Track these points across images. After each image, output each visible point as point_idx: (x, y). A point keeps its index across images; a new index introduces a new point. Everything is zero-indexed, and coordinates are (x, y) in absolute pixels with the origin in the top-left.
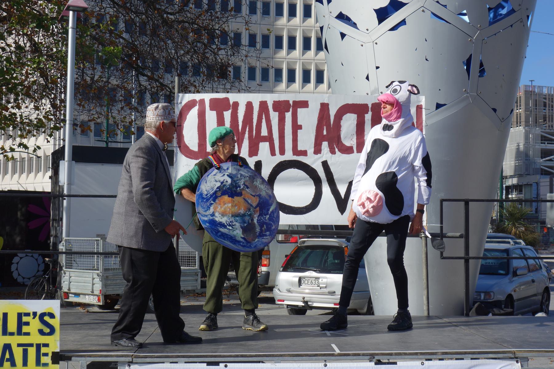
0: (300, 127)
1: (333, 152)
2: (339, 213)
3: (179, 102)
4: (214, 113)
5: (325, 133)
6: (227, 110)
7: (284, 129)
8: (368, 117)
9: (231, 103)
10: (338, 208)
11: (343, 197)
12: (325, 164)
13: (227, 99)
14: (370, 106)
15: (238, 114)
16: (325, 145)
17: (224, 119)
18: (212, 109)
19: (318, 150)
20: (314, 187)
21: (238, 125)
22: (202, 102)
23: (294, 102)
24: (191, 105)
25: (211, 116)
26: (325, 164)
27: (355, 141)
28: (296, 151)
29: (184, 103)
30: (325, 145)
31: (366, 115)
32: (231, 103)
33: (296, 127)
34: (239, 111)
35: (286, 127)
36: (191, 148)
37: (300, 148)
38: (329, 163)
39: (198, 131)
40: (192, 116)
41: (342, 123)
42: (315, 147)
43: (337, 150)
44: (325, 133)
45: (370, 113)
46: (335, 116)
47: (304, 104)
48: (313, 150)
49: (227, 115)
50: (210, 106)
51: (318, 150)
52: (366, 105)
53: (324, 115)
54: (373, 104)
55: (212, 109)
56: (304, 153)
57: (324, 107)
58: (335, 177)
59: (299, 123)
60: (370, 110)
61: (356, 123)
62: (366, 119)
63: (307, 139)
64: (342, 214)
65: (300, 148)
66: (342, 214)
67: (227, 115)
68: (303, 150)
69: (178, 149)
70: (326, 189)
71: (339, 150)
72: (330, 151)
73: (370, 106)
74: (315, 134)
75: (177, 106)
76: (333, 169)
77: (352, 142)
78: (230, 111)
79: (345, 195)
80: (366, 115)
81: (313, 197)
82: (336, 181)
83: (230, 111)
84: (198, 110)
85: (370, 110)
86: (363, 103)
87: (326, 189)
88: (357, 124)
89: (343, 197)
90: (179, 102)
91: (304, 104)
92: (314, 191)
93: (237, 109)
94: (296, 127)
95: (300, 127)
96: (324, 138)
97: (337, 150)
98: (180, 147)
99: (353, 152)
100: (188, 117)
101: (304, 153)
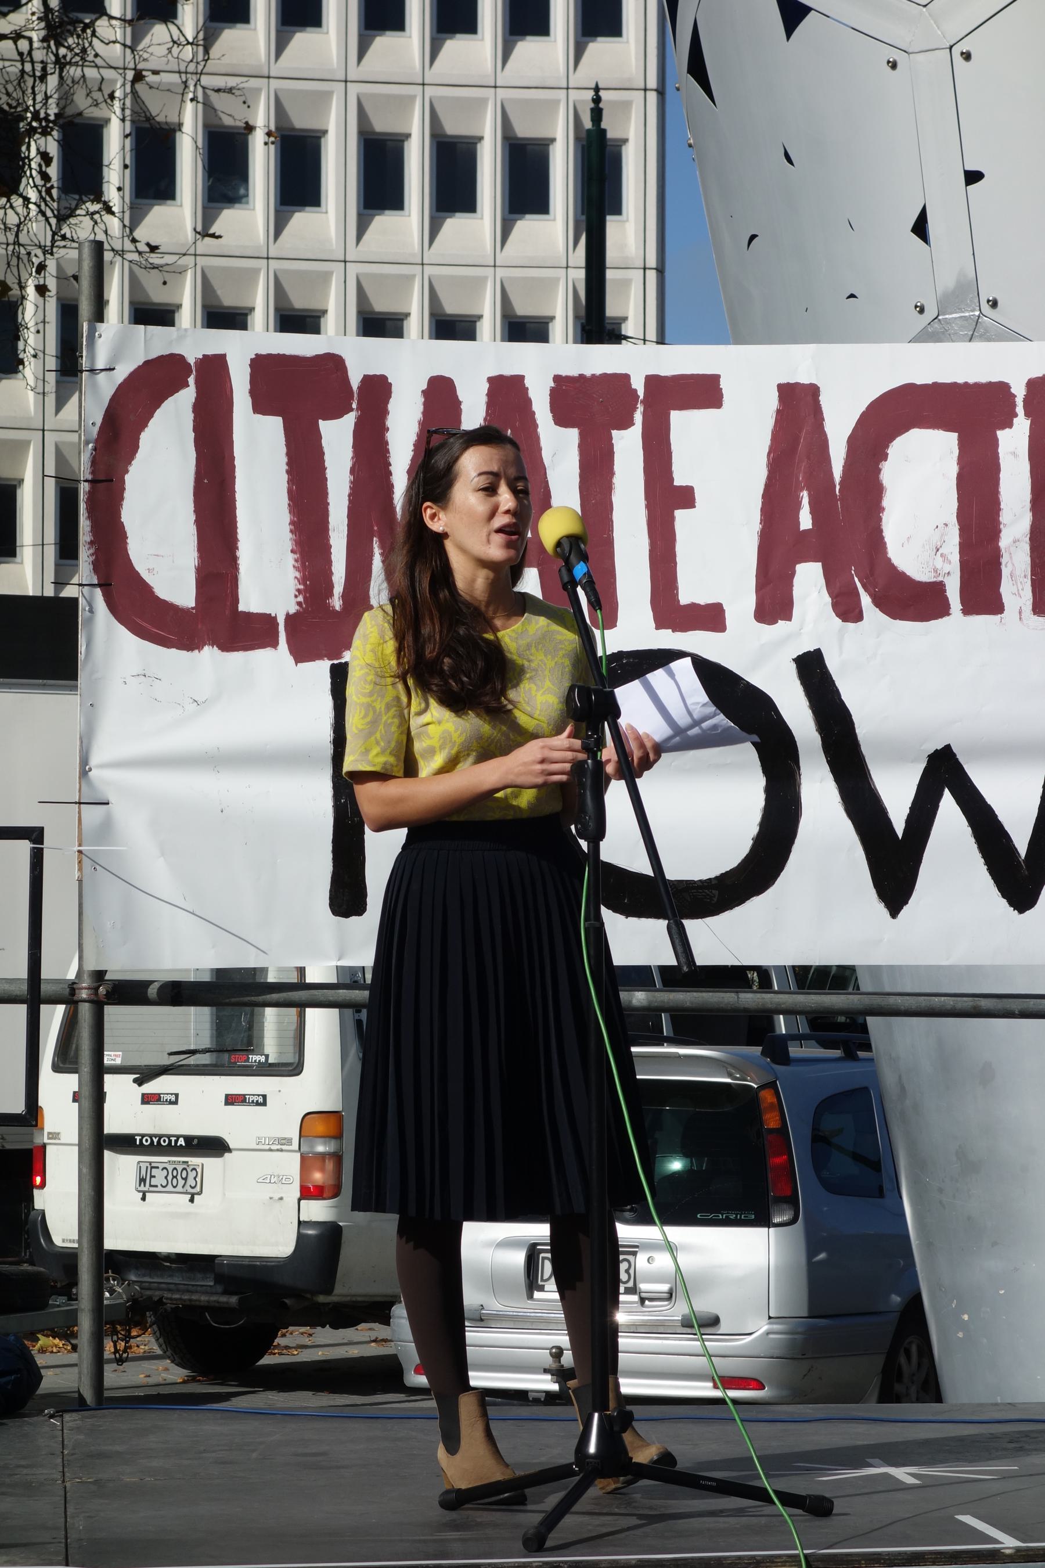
0: (686, 498)
1: (847, 609)
2: (881, 909)
3: (100, 364)
4: (274, 424)
5: (806, 521)
6: (337, 413)
7: (608, 507)
8: (1014, 443)
9: (355, 382)
10: (876, 885)
11: (899, 827)
12: (812, 670)
13: (334, 364)
14: (1019, 391)
15: (390, 436)
16: (809, 580)
17: (322, 454)
18: (261, 406)
19: (774, 604)
20: (762, 781)
21: (389, 488)
22: (214, 369)
23: (652, 381)
24: (158, 379)
25: (259, 443)
26: (812, 670)
27: (955, 558)
28: (669, 611)
29: (122, 373)
30: (809, 580)
31: (1000, 434)
32: (355, 382)
33: (666, 498)
34: (390, 422)
35: (616, 499)
36: (163, 592)
37: (685, 597)
38: (832, 664)
39: (197, 511)
40: (166, 444)
41: (890, 472)
42: (760, 587)
43: (866, 600)
44: (806, 521)
45: (1022, 424)
46: (852, 441)
47: (704, 392)
48: (750, 601)
49: (337, 437)
50: (253, 393)
51: (774, 604)
52: (1000, 391)
53: (796, 440)
54: (1035, 386)
55: (261, 406)
56: (711, 617)
57: (798, 405)
58: (862, 731)
59: (679, 481)
60: (1020, 409)
61: (953, 469)
62: (1001, 450)
63: (719, 554)
64: (894, 910)
65: (685, 597)
66: (894, 910)
67: (337, 437)
68: (702, 601)
69: (98, 592)
70: (819, 791)
71: (879, 602)
72: (835, 606)
73: (1019, 391)
74: (756, 526)
75: (95, 386)
76: (851, 693)
77: (939, 563)
78: (349, 421)
79: (907, 822)
80: (1002, 435)
81: (755, 830)
82: (864, 749)
83: (349, 421)
84: (198, 408)
85: (1020, 409)
86: (984, 380)
87: (819, 791)
88: (960, 477)
89: (899, 827)
90: (100, 364)
91: (704, 392)
92: (762, 803)
93: (384, 413)
94: (666, 498)
95: (686, 498)
96: (805, 548)
97: (866, 600)
98: (104, 585)
99: (942, 609)
100: (145, 437)
101: (711, 617)
